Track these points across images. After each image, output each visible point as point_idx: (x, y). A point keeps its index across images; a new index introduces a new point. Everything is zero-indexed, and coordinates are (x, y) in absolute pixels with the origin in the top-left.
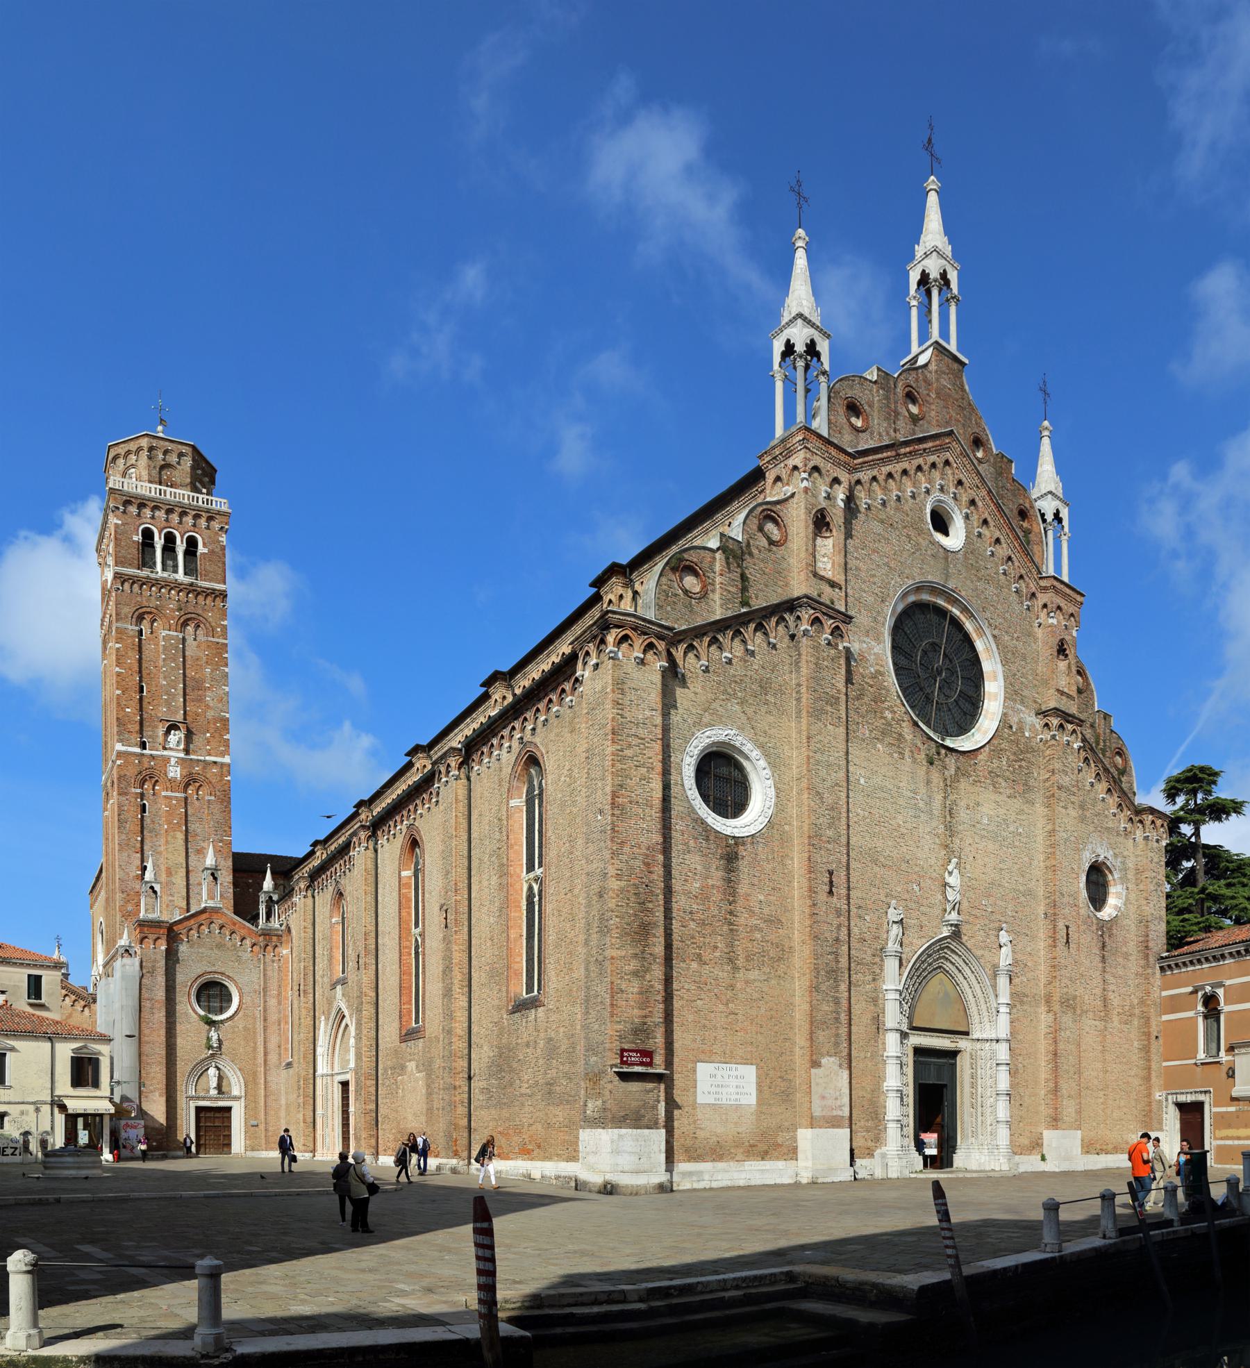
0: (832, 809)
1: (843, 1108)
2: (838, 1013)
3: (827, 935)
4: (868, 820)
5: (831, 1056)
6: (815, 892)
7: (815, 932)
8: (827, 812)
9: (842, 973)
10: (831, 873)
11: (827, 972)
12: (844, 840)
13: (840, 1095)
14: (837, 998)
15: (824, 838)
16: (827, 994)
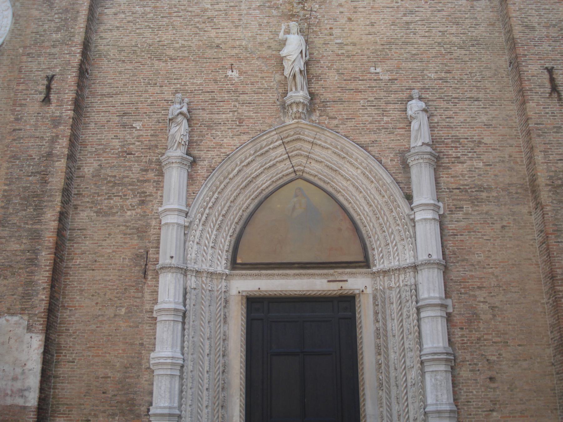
0: (66, 11)
1: (26, 393)
2: (35, 252)
3: (33, 152)
4: (152, 15)
5: (13, 314)
6: (21, 105)
7: (11, 151)
8: (56, 16)
9: (51, 196)
10: (50, 79)
11: (21, 199)
12: (79, 39)
13: (23, 373)
14: (36, 231)
15: (46, 44)
16: (20, 226)
